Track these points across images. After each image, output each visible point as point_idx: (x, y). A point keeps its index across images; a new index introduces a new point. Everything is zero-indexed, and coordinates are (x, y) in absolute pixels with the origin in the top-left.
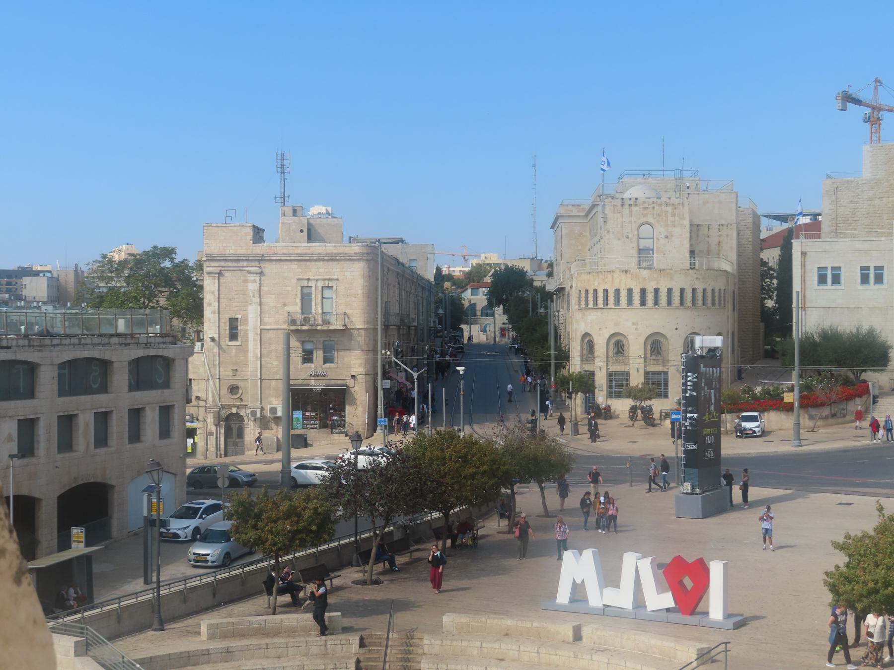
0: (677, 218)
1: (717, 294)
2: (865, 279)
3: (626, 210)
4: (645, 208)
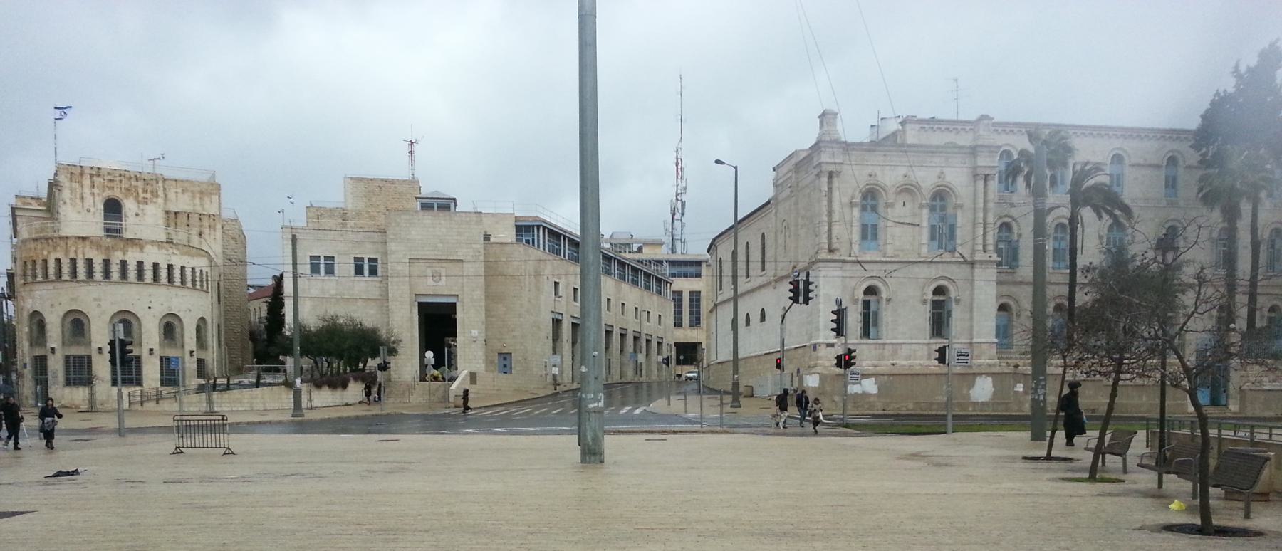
0: (148, 195)
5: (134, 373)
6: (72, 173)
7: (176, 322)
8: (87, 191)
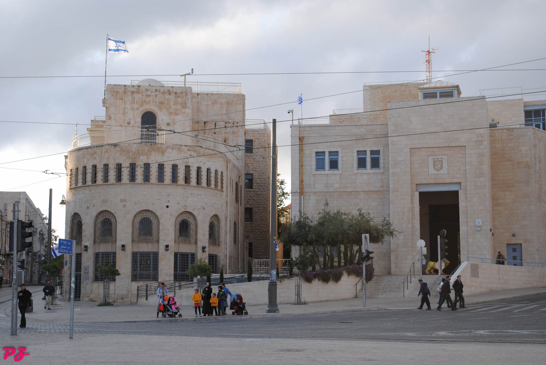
1: (213, 175)
2: (362, 163)
3: (129, 98)
4: (148, 96)
5: (152, 269)
6: (117, 92)
7: (191, 220)
8: (128, 106)
